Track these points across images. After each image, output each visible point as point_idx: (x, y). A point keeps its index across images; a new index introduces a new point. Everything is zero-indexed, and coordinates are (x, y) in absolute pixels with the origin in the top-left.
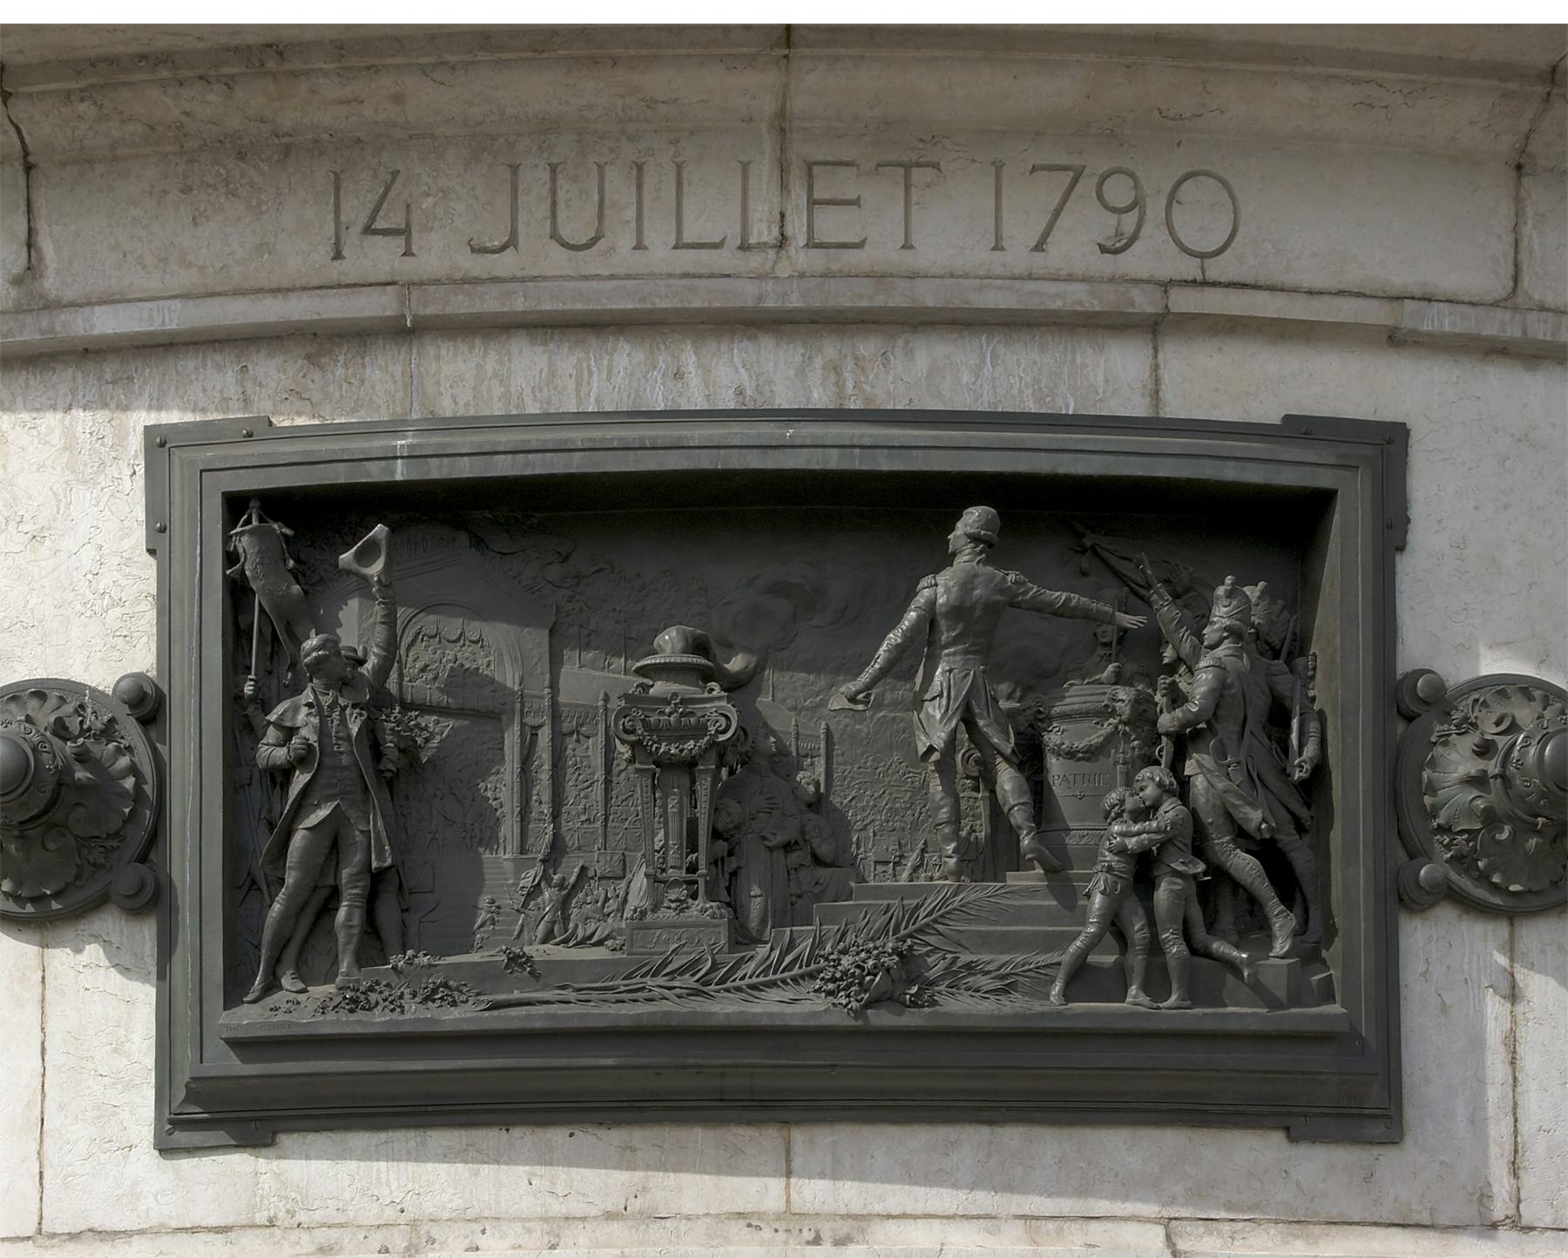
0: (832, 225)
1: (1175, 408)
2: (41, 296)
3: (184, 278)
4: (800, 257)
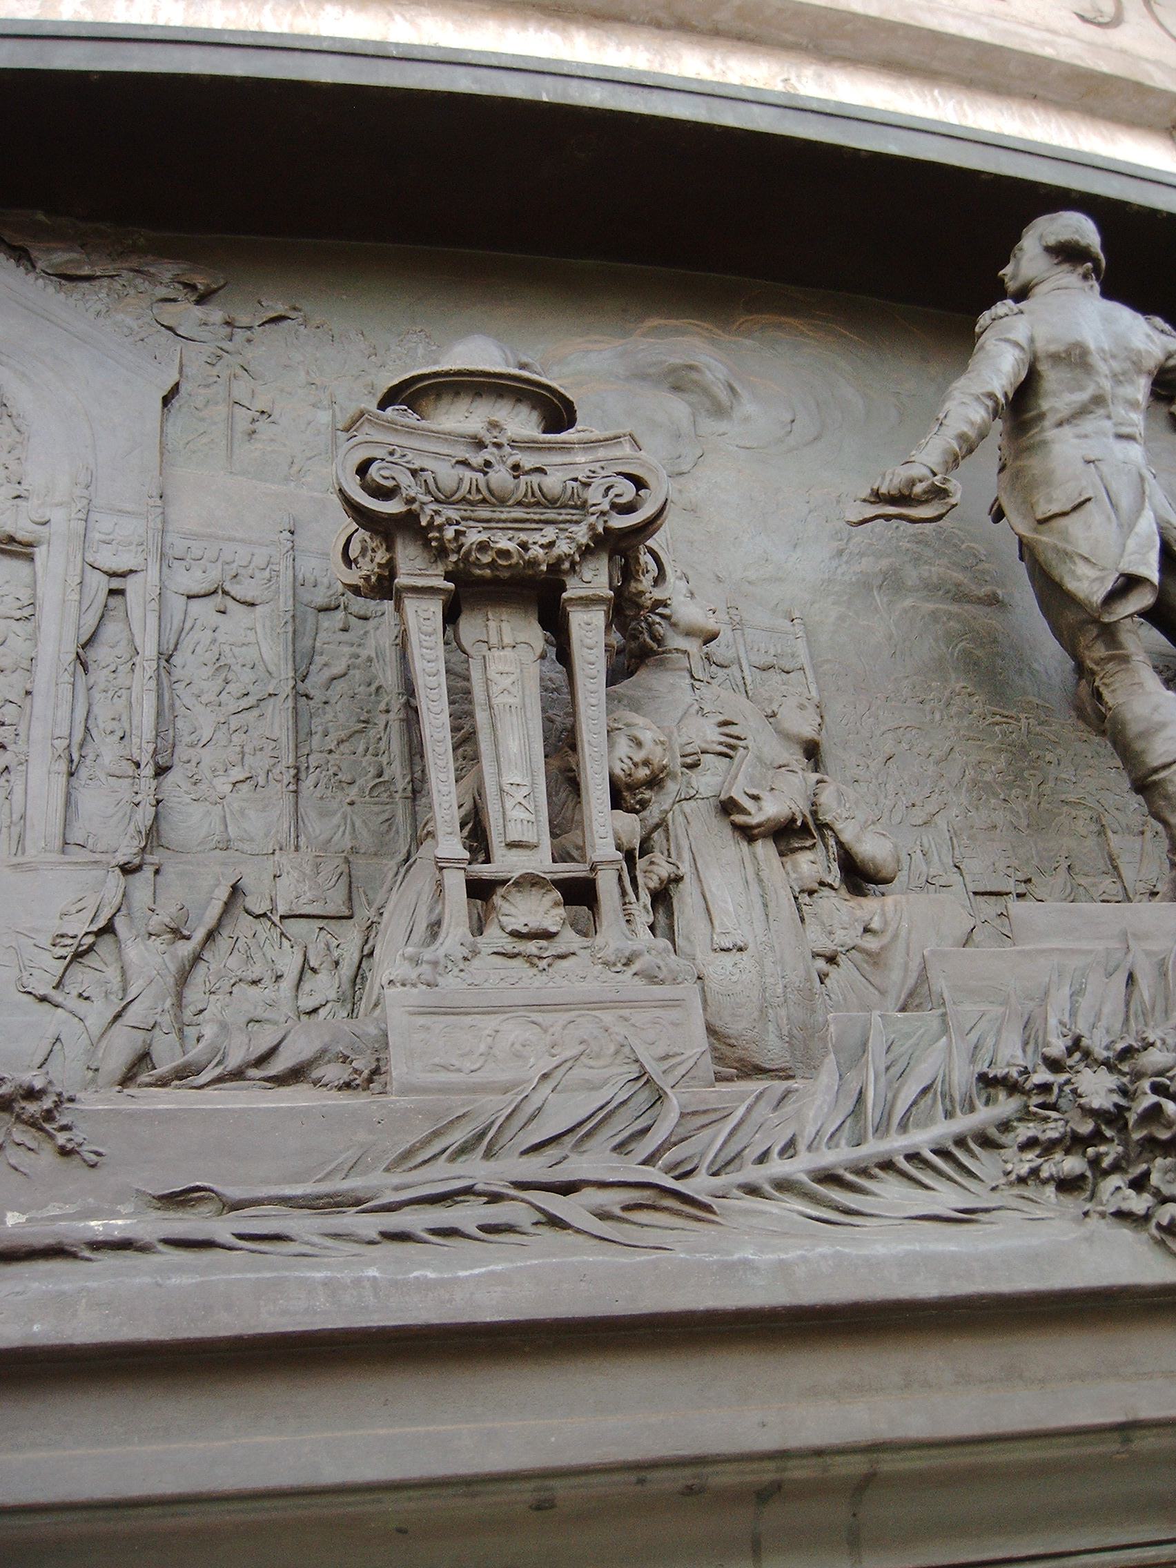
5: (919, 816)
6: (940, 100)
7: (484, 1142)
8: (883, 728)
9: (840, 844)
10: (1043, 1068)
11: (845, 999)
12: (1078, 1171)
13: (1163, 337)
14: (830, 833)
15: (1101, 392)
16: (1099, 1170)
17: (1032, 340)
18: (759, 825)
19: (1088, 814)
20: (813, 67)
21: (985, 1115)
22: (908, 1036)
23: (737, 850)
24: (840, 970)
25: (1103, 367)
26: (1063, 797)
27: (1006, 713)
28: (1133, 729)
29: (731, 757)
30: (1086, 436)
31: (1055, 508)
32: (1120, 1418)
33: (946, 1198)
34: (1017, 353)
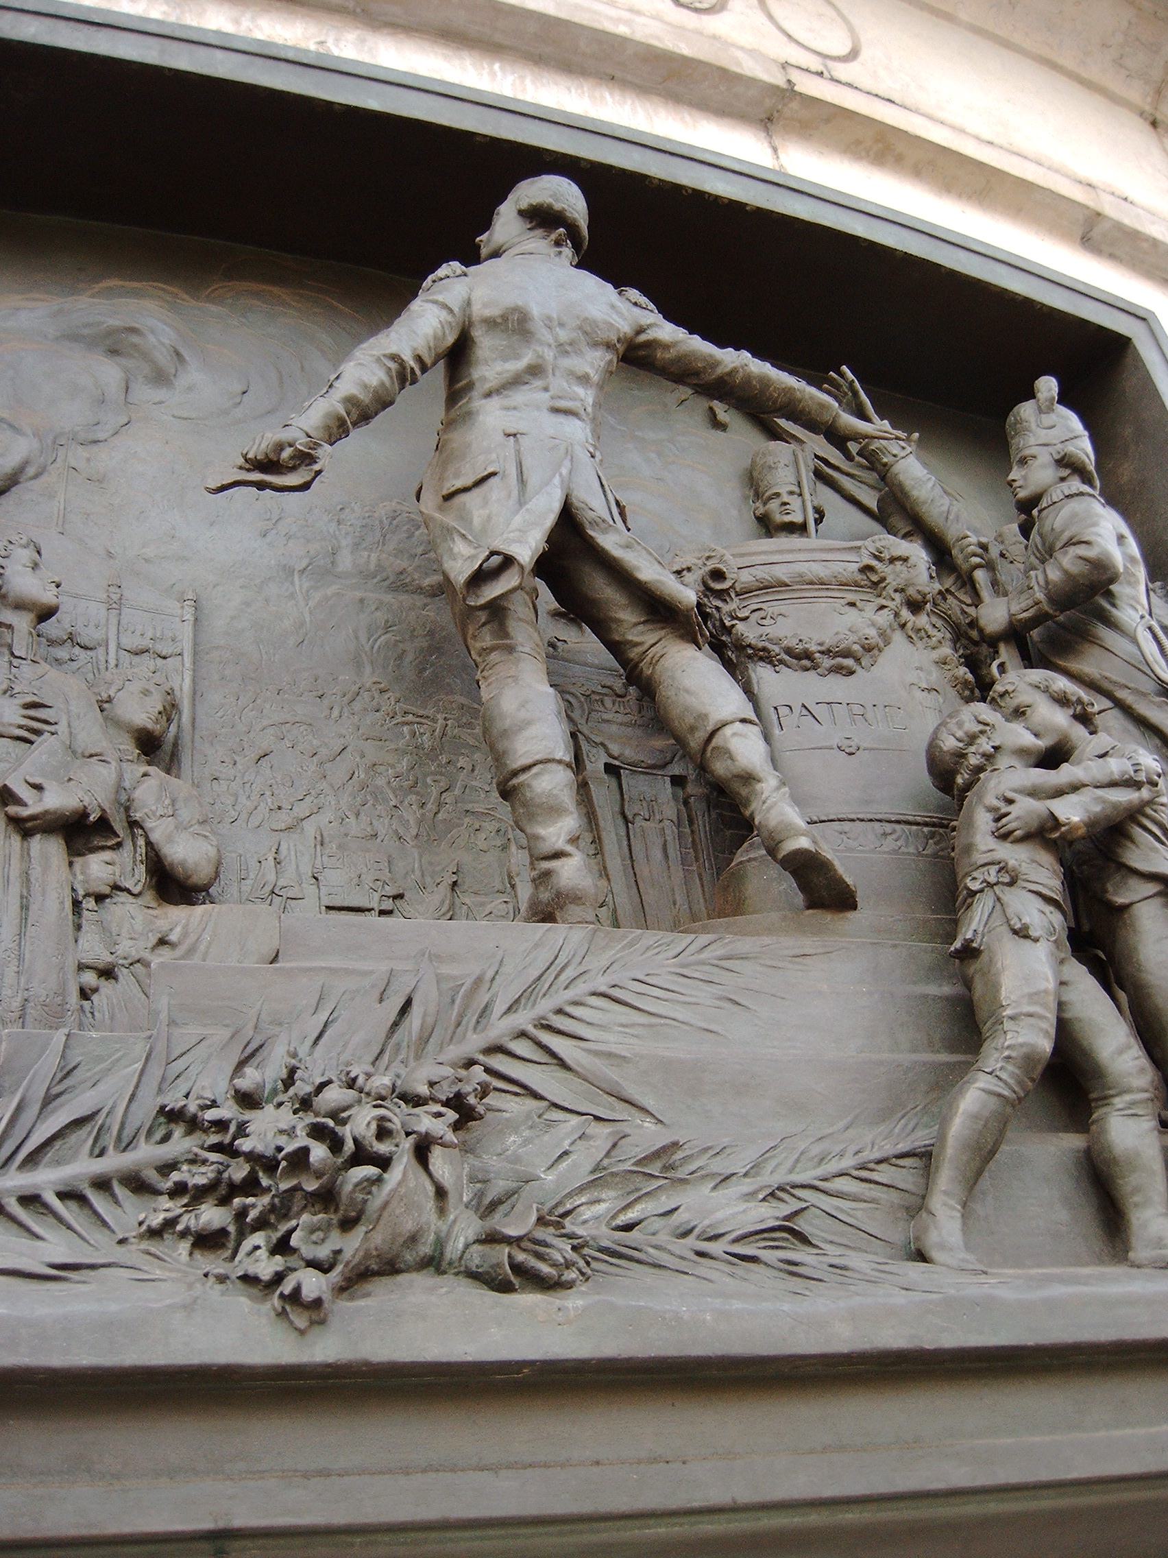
5: (283, 819)
6: (499, 74)
8: (266, 722)
9: (149, 844)
10: (231, 1102)
11: (112, 1018)
12: (216, 1225)
13: (636, 310)
14: (140, 831)
15: (540, 361)
16: (244, 1225)
17: (469, 303)
18: (33, 818)
19: (496, 825)
20: (358, 32)
21: (146, 1153)
22: (100, 1059)
24: (118, 986)
25: (545, 335)
26: (469, 807)
27: (421, 712)
28: (499, 725)
29: (32, 743)
30: (515, 408)
31: (459, 484)
32: (208, 1525)
33: (56, 1247)
34: (444, 315)
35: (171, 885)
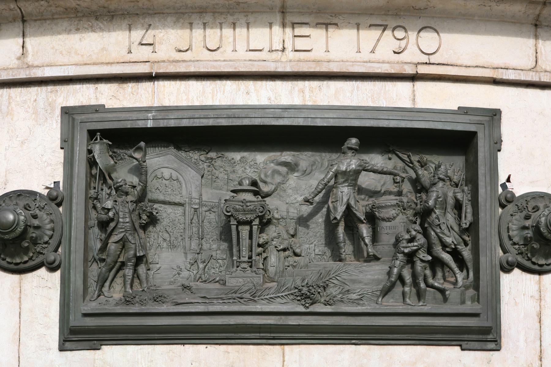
0: (301, 44)
1: (420, 105)
2: (27, 64)
3: (76, 59)
4: (290, 54)
7: (235, 292)
21: (293, 291)
23: (275, 252)
33: (285, 301)
35: (296, 255)
